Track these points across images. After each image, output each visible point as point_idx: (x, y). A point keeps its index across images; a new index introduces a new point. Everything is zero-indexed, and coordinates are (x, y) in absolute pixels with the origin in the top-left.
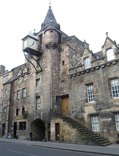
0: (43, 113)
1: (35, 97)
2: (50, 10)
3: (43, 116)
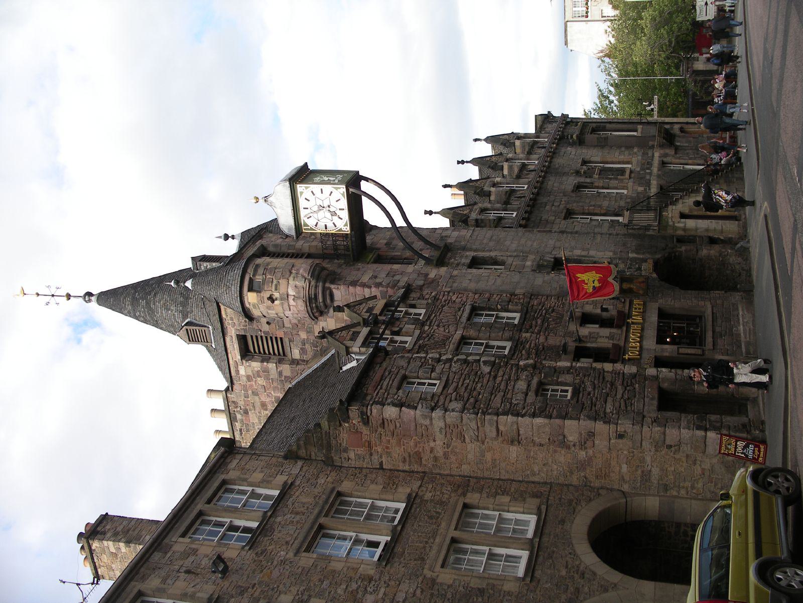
0: (633, 252)
1: (548, 273)
2: (113, 298)
3: (644, 253)
